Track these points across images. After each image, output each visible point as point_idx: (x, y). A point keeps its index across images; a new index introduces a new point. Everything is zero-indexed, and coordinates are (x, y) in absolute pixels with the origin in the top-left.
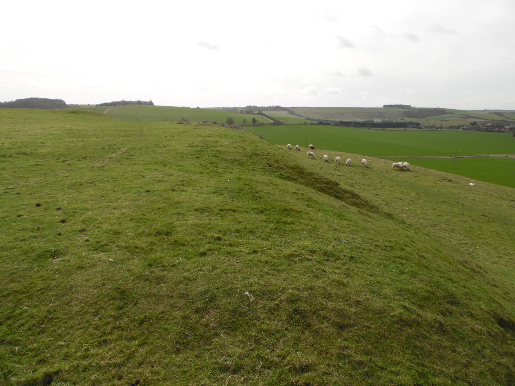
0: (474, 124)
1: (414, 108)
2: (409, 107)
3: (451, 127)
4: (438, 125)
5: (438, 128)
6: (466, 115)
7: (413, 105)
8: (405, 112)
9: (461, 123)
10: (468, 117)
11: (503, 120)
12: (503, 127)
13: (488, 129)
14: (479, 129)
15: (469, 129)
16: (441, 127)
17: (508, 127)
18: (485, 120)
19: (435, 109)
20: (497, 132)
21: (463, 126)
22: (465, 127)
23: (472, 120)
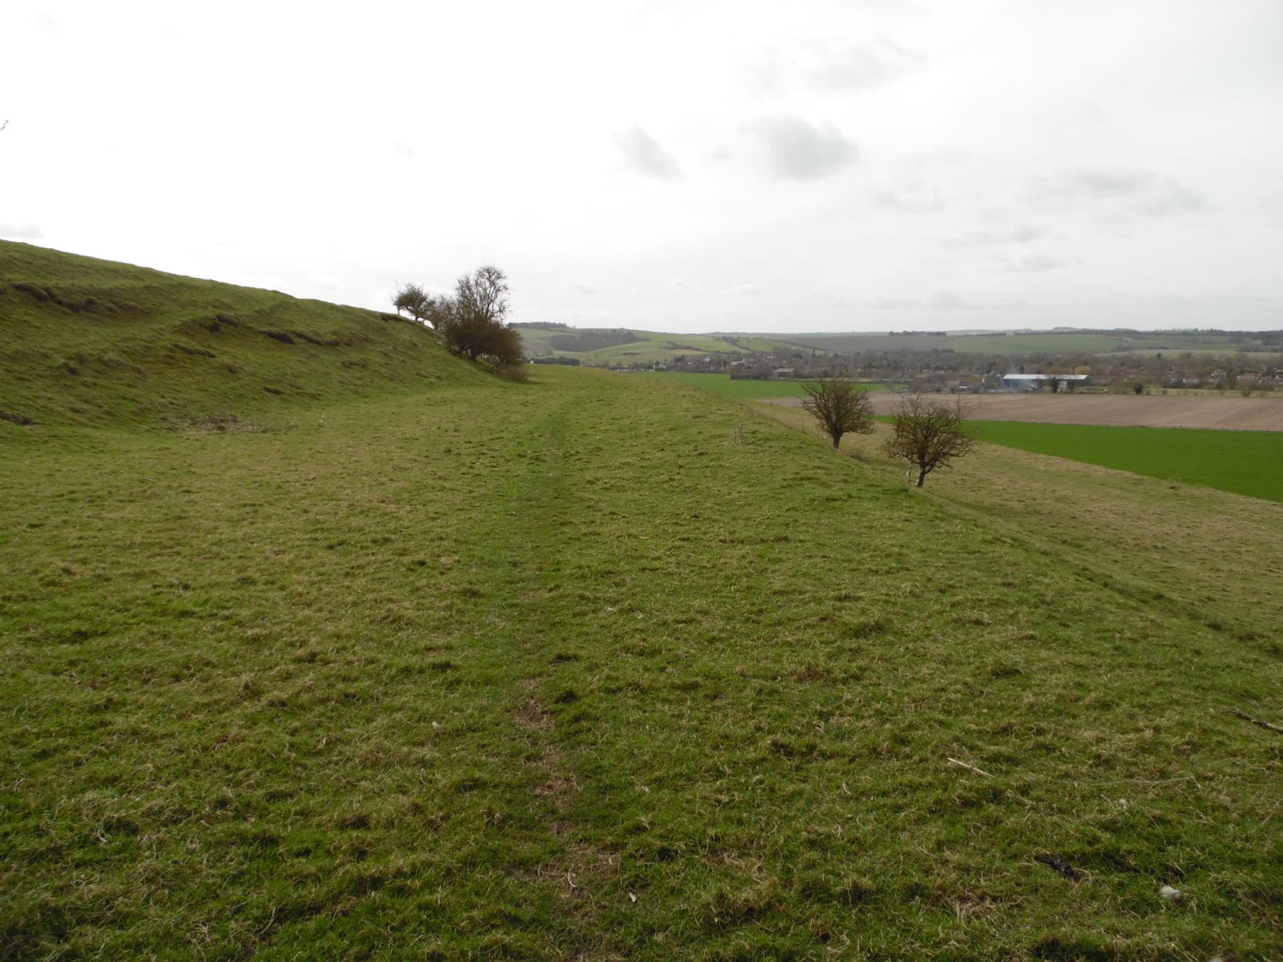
0: (681, 359)
1: (574, 330)
2: (562, 327)
3: (637, 367)
4: (612, 364)
5: (613, 369)
6: (672, 342)
7: (570, 324)
8: (553, 338)
9: (661, 358)
10: (676, 347)
11: (734, 353)
12: (726, 363)
13: (700, 367)
14: (684, 369)
15: (668, 369)
16: (619, 367)
17: (734, 363)
18: (696, 353)
19: (614, 330)
20: (713, 372)
21: (658, 363)
22: (661, 366)
23: (679, 353)
